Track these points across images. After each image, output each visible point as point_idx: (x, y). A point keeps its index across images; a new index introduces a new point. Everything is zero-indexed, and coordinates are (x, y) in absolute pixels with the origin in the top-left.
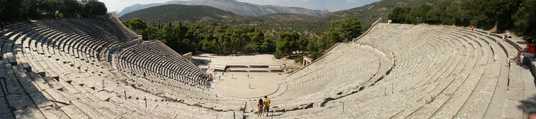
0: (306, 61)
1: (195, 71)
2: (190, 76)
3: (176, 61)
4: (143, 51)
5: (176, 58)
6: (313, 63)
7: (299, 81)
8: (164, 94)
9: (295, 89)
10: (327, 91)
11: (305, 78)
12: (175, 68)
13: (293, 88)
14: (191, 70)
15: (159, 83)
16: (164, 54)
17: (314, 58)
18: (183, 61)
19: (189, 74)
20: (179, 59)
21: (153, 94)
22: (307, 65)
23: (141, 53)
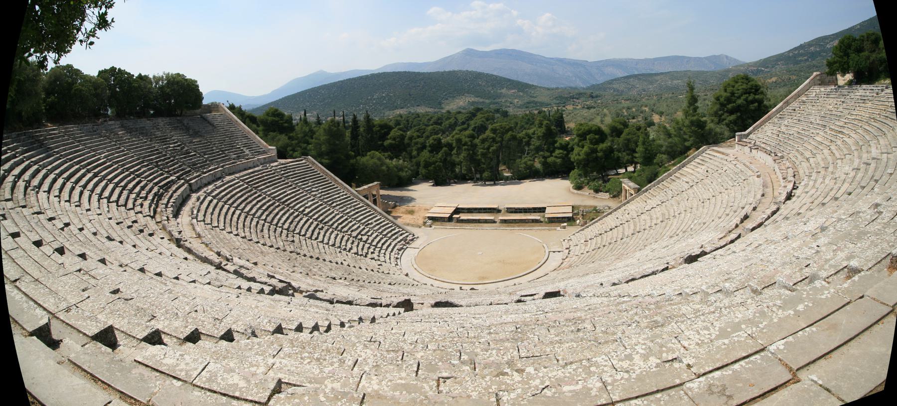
1: (378, 224)
3: (339, 203)
4: (269, 182)
5: (343, 196)
12: (334, 217)
14: (370, 222)
16: (316, 187)
20: (349, 197)
23: (263, 187)
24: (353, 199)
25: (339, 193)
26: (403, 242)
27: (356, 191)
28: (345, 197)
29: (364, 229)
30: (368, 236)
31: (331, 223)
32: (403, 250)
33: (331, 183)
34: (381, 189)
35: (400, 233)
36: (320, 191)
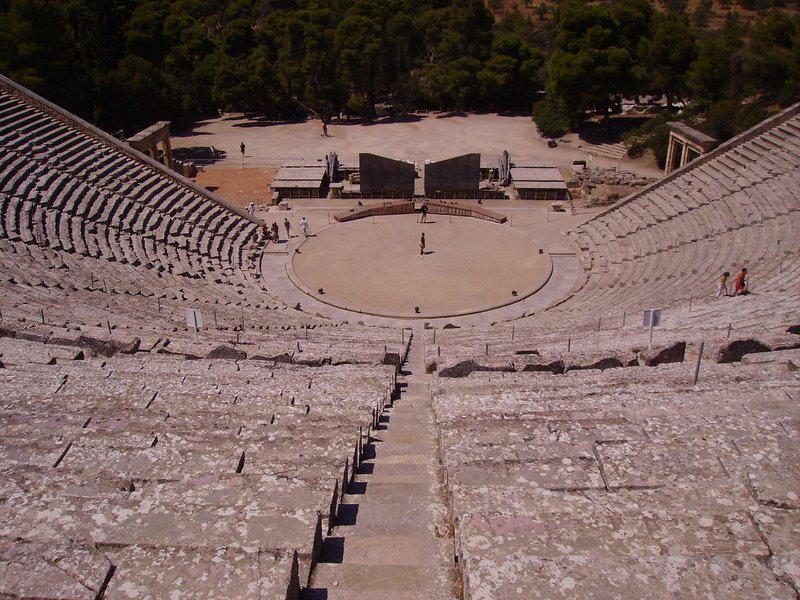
0: (678, 147)
1: (193, 210)
2: (173, 235)
3: (100, 172)
5: (101, 156)
6: (713, 156)
7: (642, 242)
8: (79, 329)
9: (622, 281)
10: (760, 313)
11: (673, 231)
12: (105, 204)
13: (616, 276)
14: (176, 206)
15: (43, 289)
17: (722, 133)
18: (133, 166)
19: (171, 223)
20: (116, 157)
21: (30, 338)
22: (683, 165)
24: (124, 162)
25: (92, 152)
26: (251, 242)
27: (132, 144)
28: (106, 158)
29: (171, 223)
30: (185, 235)
31: (105, 216)
32: (258, 259)
33: (66, 130)
34: (173, 136)
35: (240, 224)
36: (51, 150)
